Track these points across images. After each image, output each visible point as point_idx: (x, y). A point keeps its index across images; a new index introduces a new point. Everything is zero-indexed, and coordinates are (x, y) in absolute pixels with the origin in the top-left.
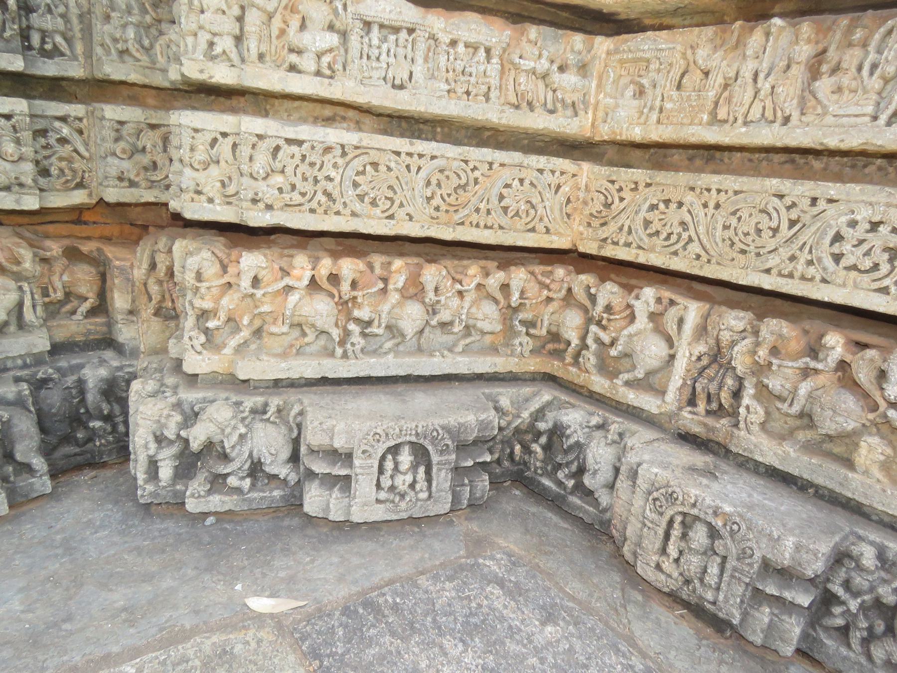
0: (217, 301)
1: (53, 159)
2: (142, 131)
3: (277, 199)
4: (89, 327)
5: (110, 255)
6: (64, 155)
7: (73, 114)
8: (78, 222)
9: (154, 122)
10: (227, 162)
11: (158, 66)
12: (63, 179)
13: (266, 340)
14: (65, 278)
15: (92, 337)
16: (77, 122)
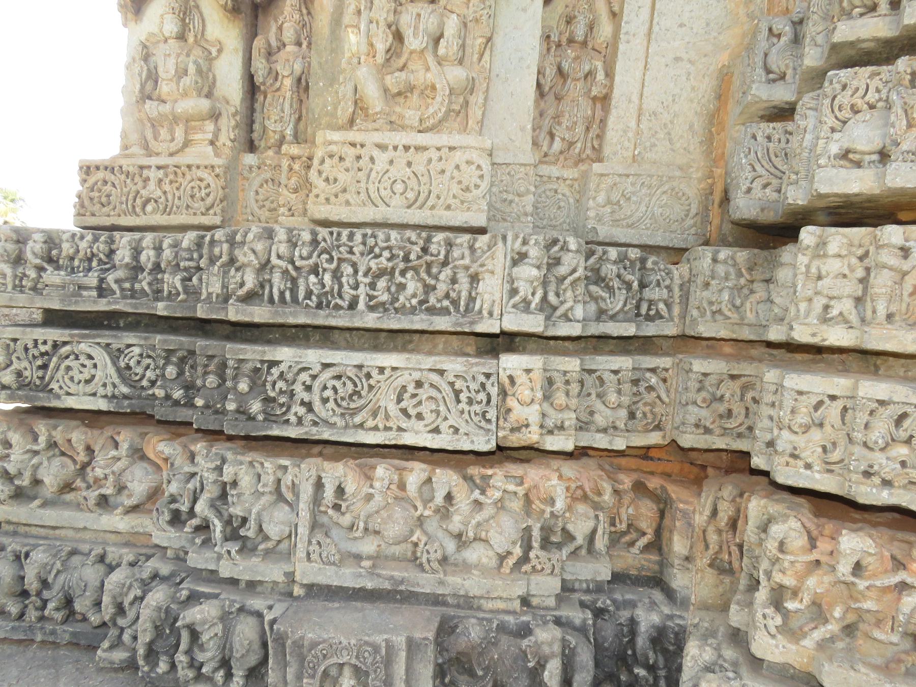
0: (801, 578)
1: (640, 404)
2: (723, 381)
3: (899, 475)
4: (643, 562)
5: (673, 496)
6: (649, 401)
7: (662, 366)
8: (646, 457)
9: (735, 373)
10: (833, 426)
11: (746, 321)
12: (645, 422)
13: (861, 642)
14: (630, 511)
15: (644, 573)
16: (664, 372)
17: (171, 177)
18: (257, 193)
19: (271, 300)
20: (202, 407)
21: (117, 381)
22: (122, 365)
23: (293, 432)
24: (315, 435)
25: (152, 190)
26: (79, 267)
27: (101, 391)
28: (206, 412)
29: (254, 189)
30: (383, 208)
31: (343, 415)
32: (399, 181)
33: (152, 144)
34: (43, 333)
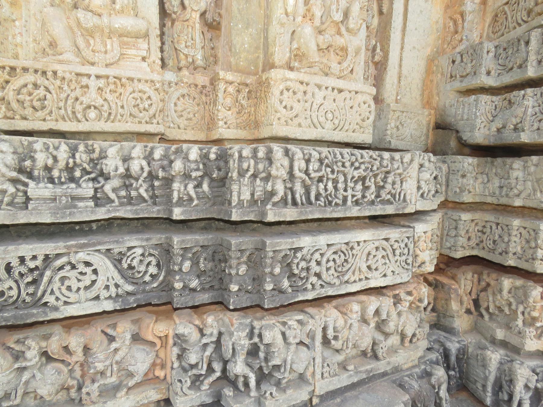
4: (431, 318)
17: (112, 87)
18: (175, 104)
19: (295, 203)
20: (238, 291)
21: (121, 282)
22: (125, 266)
23: (310, 296)
24: (324, 294)
25: (92, 97)
26: (60, 178)
27: (104, 294)
28: (241, 294)
29: (173, 102)
30: (320, 129)
31: (338, 277)
32: (329, 112)
33: (87, 53)
34: (31, 249)
